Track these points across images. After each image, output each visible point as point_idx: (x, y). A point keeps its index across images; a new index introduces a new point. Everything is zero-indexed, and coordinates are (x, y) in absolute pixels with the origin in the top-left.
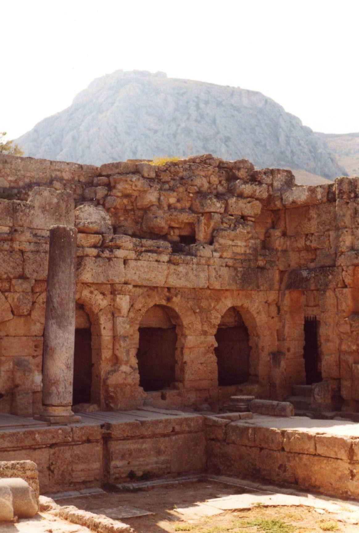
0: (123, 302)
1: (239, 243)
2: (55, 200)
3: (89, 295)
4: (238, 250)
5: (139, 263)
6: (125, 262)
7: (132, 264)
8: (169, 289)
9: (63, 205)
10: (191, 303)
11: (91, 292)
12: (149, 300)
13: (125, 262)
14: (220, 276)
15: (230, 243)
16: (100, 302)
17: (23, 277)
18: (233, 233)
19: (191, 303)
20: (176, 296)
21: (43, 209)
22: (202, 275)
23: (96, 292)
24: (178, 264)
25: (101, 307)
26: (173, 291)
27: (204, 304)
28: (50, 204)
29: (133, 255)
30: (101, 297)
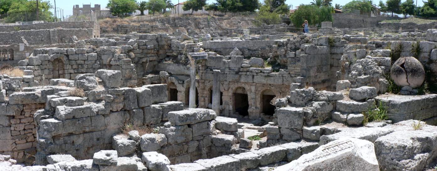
0: (253, 88)
1: (298, 68)
2: (235, 59)
4: (297, 71)
5: (258, 77)
6: (253, 76)
7: (255, 77)
8: (270, 85)
9: (238, 61)
10: (278, 89)
12: (263, 88)
14: (288, 81)
15: (294, 68)
17: (226, 81)
18: (294, 65)
19: (278, 89)
21: (233, 62)
22: (280, 80)
26: (272, 85)
27: (283, 90)
28: (234, 60)
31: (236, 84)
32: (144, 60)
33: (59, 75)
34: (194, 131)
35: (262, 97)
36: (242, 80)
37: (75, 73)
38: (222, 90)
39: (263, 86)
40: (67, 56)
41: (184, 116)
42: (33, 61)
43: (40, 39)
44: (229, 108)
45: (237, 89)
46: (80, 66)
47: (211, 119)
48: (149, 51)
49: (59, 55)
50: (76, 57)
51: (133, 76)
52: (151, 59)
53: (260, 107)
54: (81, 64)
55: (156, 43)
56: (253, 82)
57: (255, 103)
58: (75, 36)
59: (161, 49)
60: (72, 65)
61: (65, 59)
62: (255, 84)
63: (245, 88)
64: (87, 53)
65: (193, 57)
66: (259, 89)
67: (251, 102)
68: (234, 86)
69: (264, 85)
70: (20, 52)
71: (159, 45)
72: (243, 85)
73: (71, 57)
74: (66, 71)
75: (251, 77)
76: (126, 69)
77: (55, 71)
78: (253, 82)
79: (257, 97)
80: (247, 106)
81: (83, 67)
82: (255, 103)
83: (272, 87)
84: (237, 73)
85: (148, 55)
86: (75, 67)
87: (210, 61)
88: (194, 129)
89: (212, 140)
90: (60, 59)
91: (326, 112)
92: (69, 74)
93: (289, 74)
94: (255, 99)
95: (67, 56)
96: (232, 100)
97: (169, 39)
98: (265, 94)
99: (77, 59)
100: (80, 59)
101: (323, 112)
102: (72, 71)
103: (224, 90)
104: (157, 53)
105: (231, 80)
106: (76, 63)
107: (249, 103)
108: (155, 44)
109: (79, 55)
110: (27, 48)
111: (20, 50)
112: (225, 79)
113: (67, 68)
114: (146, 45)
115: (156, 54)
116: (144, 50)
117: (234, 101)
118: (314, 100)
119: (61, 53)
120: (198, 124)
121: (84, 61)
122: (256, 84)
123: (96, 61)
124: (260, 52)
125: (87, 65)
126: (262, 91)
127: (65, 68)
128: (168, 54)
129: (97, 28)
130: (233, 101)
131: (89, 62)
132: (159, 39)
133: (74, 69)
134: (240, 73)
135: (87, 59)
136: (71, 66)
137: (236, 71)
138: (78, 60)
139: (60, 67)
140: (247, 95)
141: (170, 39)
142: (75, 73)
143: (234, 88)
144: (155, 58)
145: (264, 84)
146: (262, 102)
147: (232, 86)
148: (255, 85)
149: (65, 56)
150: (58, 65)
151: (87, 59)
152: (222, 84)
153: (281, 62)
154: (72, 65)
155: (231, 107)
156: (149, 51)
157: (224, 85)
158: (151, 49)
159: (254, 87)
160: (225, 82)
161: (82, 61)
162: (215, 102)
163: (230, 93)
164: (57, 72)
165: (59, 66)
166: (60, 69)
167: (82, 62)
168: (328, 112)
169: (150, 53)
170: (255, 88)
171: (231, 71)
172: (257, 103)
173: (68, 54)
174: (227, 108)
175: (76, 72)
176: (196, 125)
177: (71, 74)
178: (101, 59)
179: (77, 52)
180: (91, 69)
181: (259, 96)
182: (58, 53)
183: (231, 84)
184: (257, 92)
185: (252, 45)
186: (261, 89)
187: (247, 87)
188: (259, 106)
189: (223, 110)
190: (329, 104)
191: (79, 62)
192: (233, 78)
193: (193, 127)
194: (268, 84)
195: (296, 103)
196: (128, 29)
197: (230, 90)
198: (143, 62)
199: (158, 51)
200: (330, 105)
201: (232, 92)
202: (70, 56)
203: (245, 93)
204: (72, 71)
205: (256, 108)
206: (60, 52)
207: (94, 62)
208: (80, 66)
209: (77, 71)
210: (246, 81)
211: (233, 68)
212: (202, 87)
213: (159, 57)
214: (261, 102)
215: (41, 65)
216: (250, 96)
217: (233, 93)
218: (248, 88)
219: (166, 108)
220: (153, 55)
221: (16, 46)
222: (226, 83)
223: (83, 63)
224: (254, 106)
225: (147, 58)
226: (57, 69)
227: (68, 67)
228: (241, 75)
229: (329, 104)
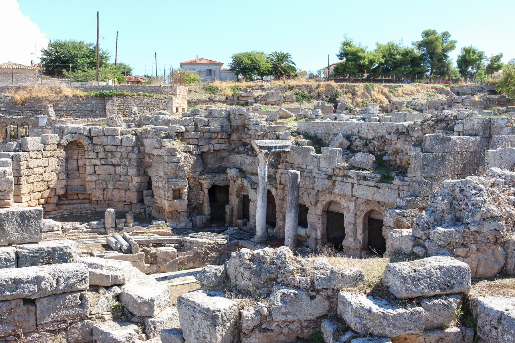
2: (329, 154)
3: (339, 200)
6: (353, 184)
8: (379, 202)
9: (331, 155)
11: (340, 198)
12: (368, 206)
13: (353, 184)
16: (344, 203)
17: (313, 189)
20: (383, 206)
23: (342, 199)
24: (379, 188)
25: (344, 206)
26: (381, 203)
28: (327, 156)
29: (355, 181)
30: (344, 201)
31: (328, 195)
32: (205, 149)
33: (78, 167)
34: (38, 312)
35: (367, 222)
36: (336, 191)
37: (101, 165)
38: (308, 205)
39: (368, 204)
40: (91, 138)
41: (6, 281)
42: (27, 144)
43: (90, 109)
44: (316, 235)
45: (330, 203)
46: (109, 154)
47: (109, 285)
48: (214, 135)
49: (76, 136)
50: (105, 140)
51: (181, 174)
52: (217, 147)
53: (361, 240)
54: (112, 152)
55: (226, 123)
56: (353, 196)
57: (355, 232)
58: (136, 108)
59: (233, 132)
60: (97, 153)
61: (85, 142)
62: (354, 198)
63: (341, 203)
64: (122, 134)
65: (261, 148)
66: (362, 208)
67: (348, 229)
68: (324, 200)
69: (367, 202)
70: (41, 127)
71: (231, 126)
72: (338, 199)
73: (95, 140)
74: (87, 161)
75: (349, 186)
76: (168, 163)
77: (72, 160)
78: (353, 196)
79: (358, 221)
80: (343, 236)
81: (114, 157)
82: (355, 232)
83: (382, 207)
84: (330, 177)
85: (214, 142)
86: (101, 155)
87: (293, 155)
88: (38, 308)
89: (92, 331)
90: (80, 143)
91: (302, 318)
92: (93, 166)
93: (409, 186)
94: (355, 224)
95: (91, 138)
96: (320, 222)
97: (247, 117)
98: (374, 216)
99: (106, 143)
100: (109, 144)
101: (290, 317)
102: (97, 162)
103: (310, 205)
104: (228, 139)
105: (319, 189)
106: (104, 149)
107: (346, 230)
108: (224, 125)
109: (109, 137)
110: (50, 122)
111: (40, 125)
112: (312, 185)
113: (90, 157)
114: (208, 125)
115: (227, 141)
116: (205, 134)
117: (325, 224)
118: (279, 280)
119: (80, 133)
120: (51, 299)
121: (116, 147)
122: (357, 198)
123: (133, 147)
124: (375, 142)
125: (120, 154)
126: (365, 211)
127: (87, 156)
128: (244, 140)
129: (181, 96)
130: (323, 224)
131: (124, 149)
132: (232, 116)
133: (101, 159)
134: (334, 178)
135: (120, 144)
136: (95, 154)
137: (328, 173)
138: (108, 145)
139: (79, 155)
140: (342, 215)
141: (249, 117)
142: (101, 165)
143: (324, 203)
144: (223, 146)
145: (370, 200)
146: (367, 231)
147: (321, 199)
148: (356, 201)
149: (87, 138)
150: (76, 152)
151: (120, 144)
152: (308, 194)
153: (401, 162)
154: (97, 153)
155: (319, 233)
156: (214, 135)
157: (311, 196)
158: (218, 133)
159: (353, 203)
160: (311, 190)
161: (113, 147)
162: (290, 224)
163: (319, 212)
164: (75, 163)
165: (78, 153)
166: (79, 157)
167: (114, 149)
168: (310, 317)
169: (216, 138)
170: (356, 205)
171: (320, 172)
172: (358, 233)
173: (92, 135)
174: (313, 235)
175: (103, 163)
176: (45, 301)
177: (95, 165)
178: (143, 145)
179: (106, 134)
180: (126, 160)
181: (362, 220)
182: (76, 133)
183: (320, 195)
184: (358, 213)
185: (366, 131)
186: (364, 209)
187: (344, 203)
188: (360, 237)
189: (308, 237)
190: (312, 298)
191: (108, 148)
192: (324, 186)
193: (38, 304)
194: (375, 201)
195: (237, 283)
196: (248, 98)
197: (319, 205)
198: (203, 152)
199: (230, 135)
200: (316, 300)
201: (321, 209)
202: (94, 138)
203: (341, 212)
204: (97, 162)
205: (355, 240)
206: (78, 132)
207: (130, 148)
208: (109, 154)
209: (105, 162)
210: (342, 193)
211: (324, 169)
212: (280, 196)
213: (230, 144)
214: (364, 231)
215: (44, 150)
216: (348, 218)
217: (323, 211)
218: (345, 205)
219: (24, 255)
220: (221, 141)
221: (33, 118)
222: (313, 193)
223: (115, 150)
224: (351, 237)
225: (210, 146)
226: (75, 157)
227: (92, 155)
228: (335, 181)
229: (312, 298)
